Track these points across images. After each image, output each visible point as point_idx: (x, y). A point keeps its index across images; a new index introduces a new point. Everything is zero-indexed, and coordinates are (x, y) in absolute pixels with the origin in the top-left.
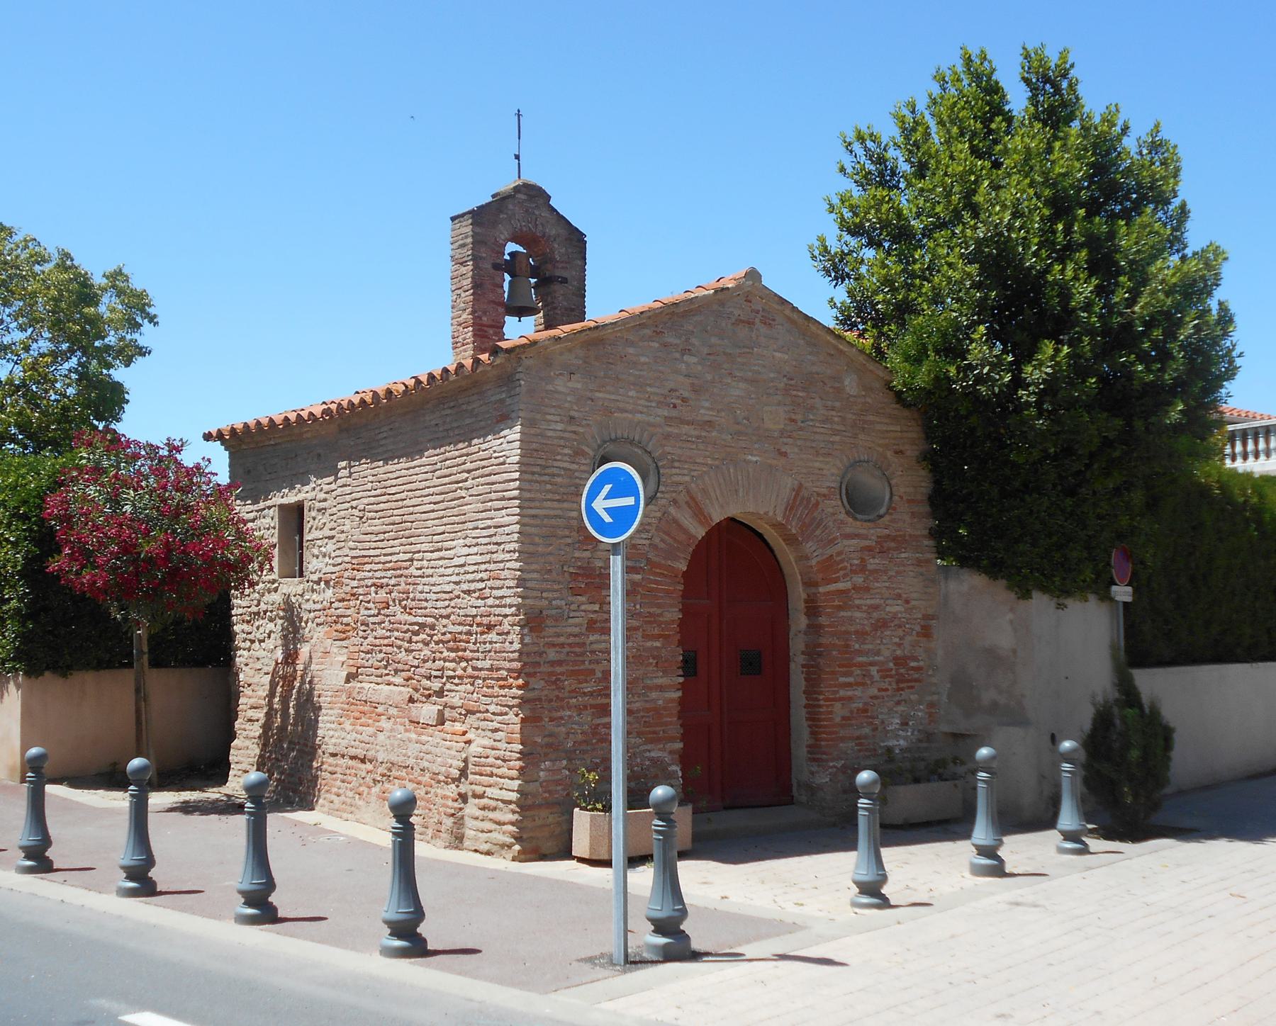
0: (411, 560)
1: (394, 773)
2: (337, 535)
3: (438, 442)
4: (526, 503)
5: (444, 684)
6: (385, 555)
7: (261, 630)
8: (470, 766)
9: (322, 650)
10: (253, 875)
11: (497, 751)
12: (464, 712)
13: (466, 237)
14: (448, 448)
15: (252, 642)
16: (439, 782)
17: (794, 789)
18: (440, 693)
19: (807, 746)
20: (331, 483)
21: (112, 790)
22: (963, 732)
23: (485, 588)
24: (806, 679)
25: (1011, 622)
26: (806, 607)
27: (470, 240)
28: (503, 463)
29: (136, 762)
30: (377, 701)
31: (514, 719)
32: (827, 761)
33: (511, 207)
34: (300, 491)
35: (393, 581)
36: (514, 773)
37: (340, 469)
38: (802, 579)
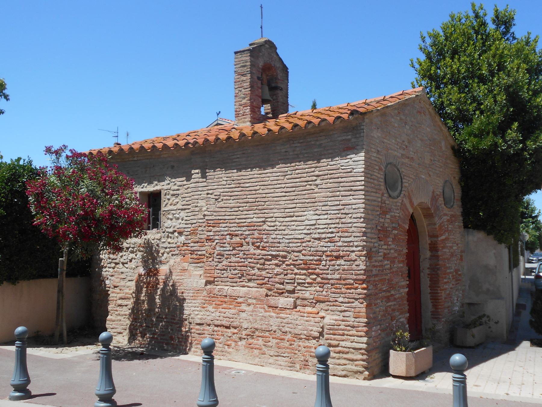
0: (264, 222)
1: (257, 333)
2: (192, 208)
3: (287, 160)
4: (367, 192)
5: (296, 287)
6: (239, 219)
7: (124, 257)
8: (325, 330)
9: (180, 268)
10: (210, 397)
11: (346, 322)
12: (314, 302)
13: (246, 62)
14: (297, 164)
15: (116, 264)
16: (301, 339)
17: (424, 332)
18: (293, 292)
19: (431, 312)
20: (184, 181)
21: (48, 348)
22: (476, 303)
23: (335, 237)
24: (430, 281)
25: (494, 254)
26: (430, 247)
27: (249, 64)
28: (351, 172)
29: (20, 329)
30: (237, 296)
31: (361, 307)
32: (441, 318)
33: (263, 50)
34: (157, 185)
35: (247, 233)
36: (363, 334)
37: (193, 174)
38: (428, 234)
